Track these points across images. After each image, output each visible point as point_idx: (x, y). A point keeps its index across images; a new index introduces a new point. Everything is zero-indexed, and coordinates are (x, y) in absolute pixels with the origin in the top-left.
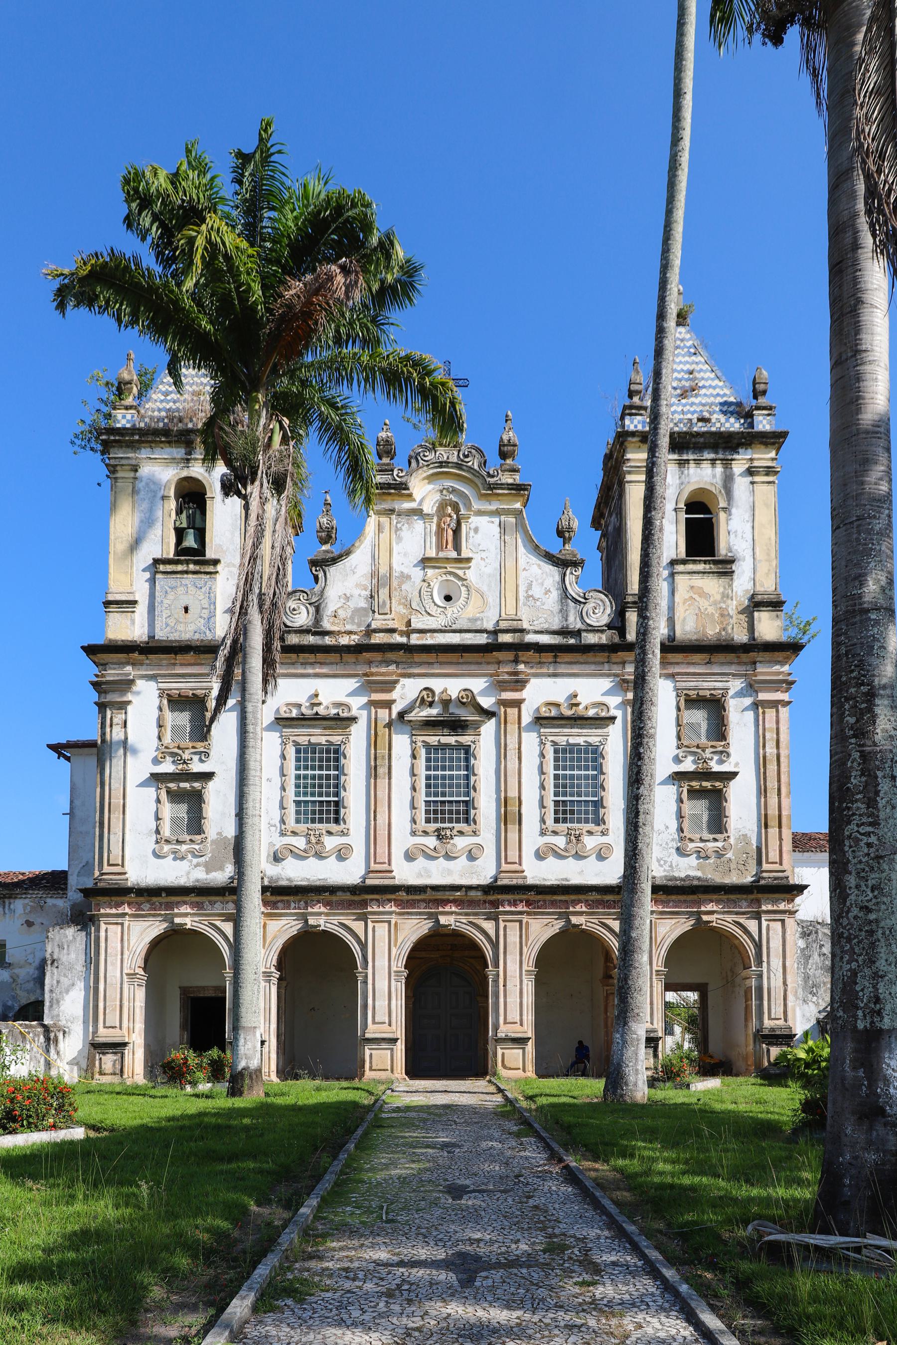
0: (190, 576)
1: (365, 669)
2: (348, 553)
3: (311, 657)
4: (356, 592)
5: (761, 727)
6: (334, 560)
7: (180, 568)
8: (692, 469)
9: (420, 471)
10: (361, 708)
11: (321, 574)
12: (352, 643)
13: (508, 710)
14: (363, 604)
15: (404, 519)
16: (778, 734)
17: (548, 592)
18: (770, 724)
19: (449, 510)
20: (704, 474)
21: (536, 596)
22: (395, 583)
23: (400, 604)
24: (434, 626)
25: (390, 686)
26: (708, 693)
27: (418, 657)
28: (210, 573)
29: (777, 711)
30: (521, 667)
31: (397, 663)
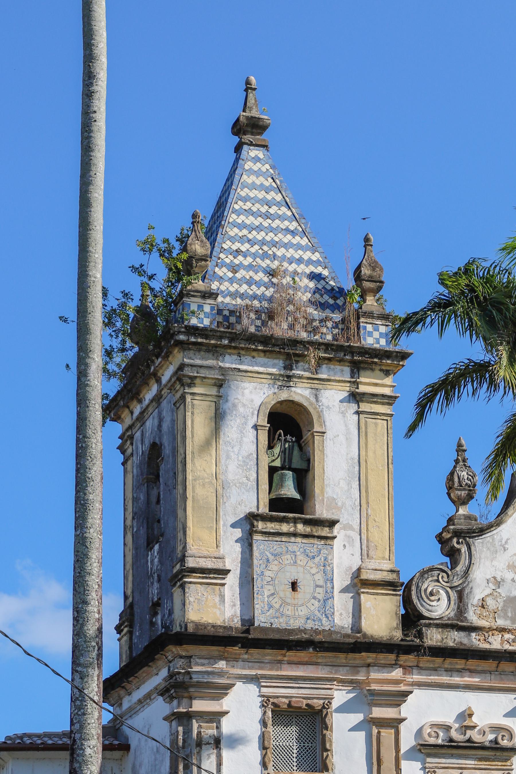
0: (299, 540)
3: (460, 663)
7: (285, 528)
11: (464, 549)
12: (507, 647)
28: (326, 538)
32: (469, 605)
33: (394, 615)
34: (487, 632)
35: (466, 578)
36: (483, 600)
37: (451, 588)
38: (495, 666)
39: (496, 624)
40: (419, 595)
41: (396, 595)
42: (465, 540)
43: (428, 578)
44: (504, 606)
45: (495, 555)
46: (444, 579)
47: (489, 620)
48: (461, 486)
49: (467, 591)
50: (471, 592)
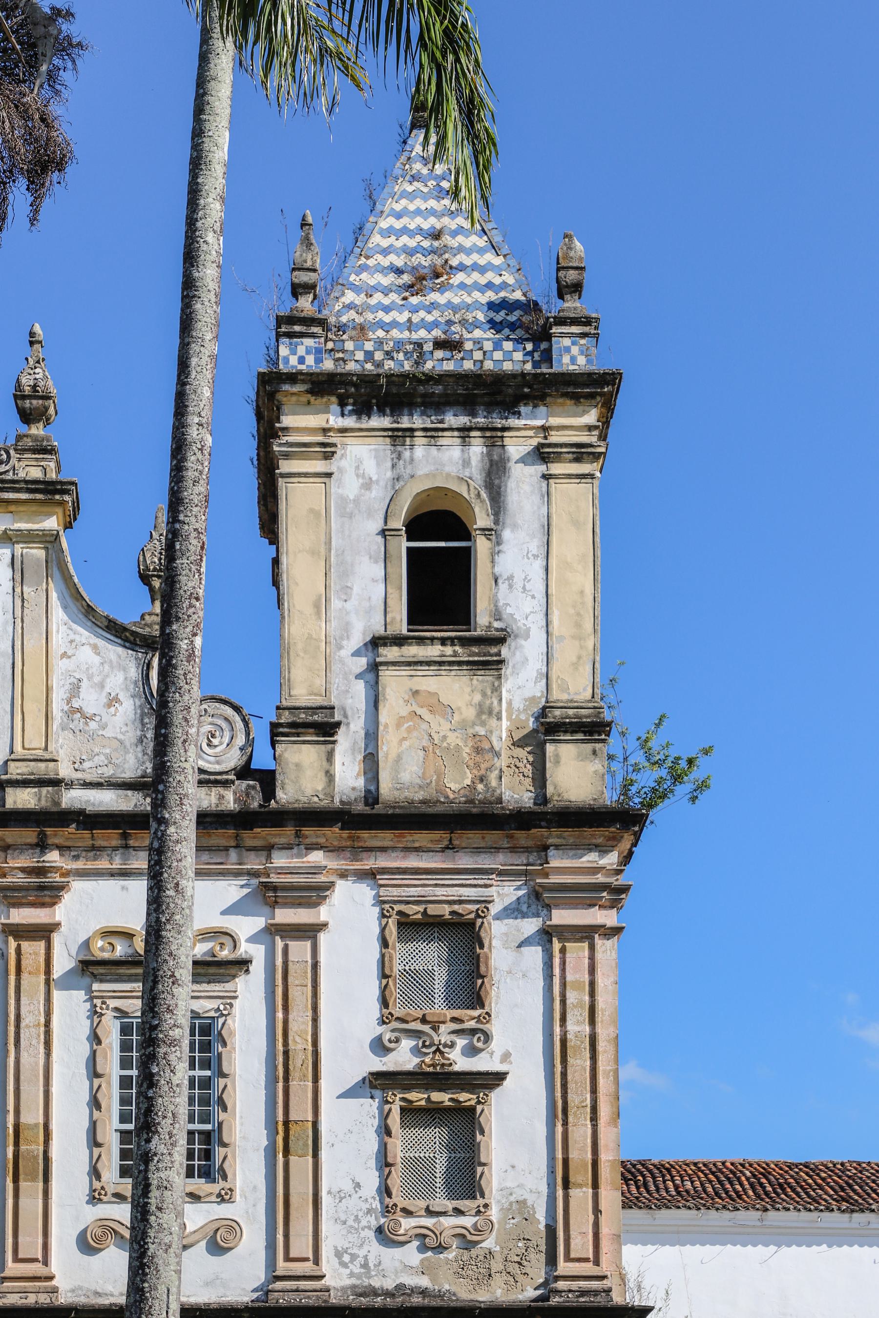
5: (557, 981)
8: (420, 450)
13: (25, 945)
16: (592, 994)
17: (113, 701)
18: (577, 973)
20: (446, 461)
21: (89, 710)
26: (445, 911)
29: (592, 948)
30: (53, 857)
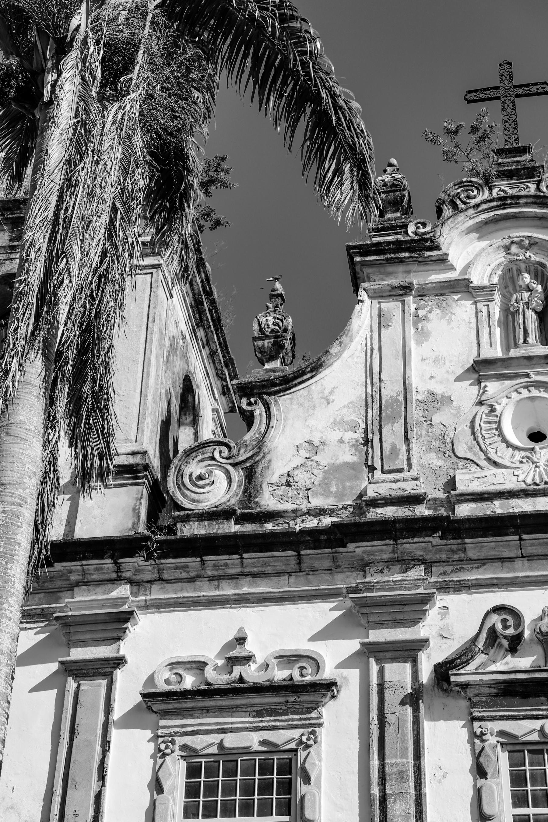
1: (355, 579)
2: (316, 368)
3: (231, 562)
4: (333, 436)
6: (287, 383)
9: (461, 217)
10: (344, 665)
11: (259, 410)
14: (348, 456)
15: (432, 302)
19: (527, 278)
22: (416, 414)
23: (429, 450)
24: (510, 484)
25: (412, 608)
27: (474, 547)
31: (428, 565)
32: (265, 486)
33: (131, 512)
34: (294, 520)
35: (260, 448)
36: (289, 476)
37: (234, 465)
38: (294, 562)
39: (309, 505)
40: (180, 482)
41: (137, 484)
42: (261, 399)
43: (196, 456)
44: (325, 478)
45: (311, 412)
46: (223, 455)
47: (298, 502)
48: (264, 334)
49: (261, 466)
50: (268, 467)
